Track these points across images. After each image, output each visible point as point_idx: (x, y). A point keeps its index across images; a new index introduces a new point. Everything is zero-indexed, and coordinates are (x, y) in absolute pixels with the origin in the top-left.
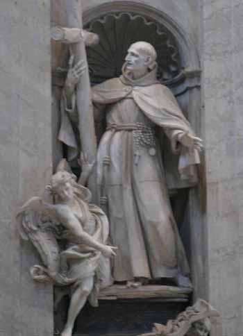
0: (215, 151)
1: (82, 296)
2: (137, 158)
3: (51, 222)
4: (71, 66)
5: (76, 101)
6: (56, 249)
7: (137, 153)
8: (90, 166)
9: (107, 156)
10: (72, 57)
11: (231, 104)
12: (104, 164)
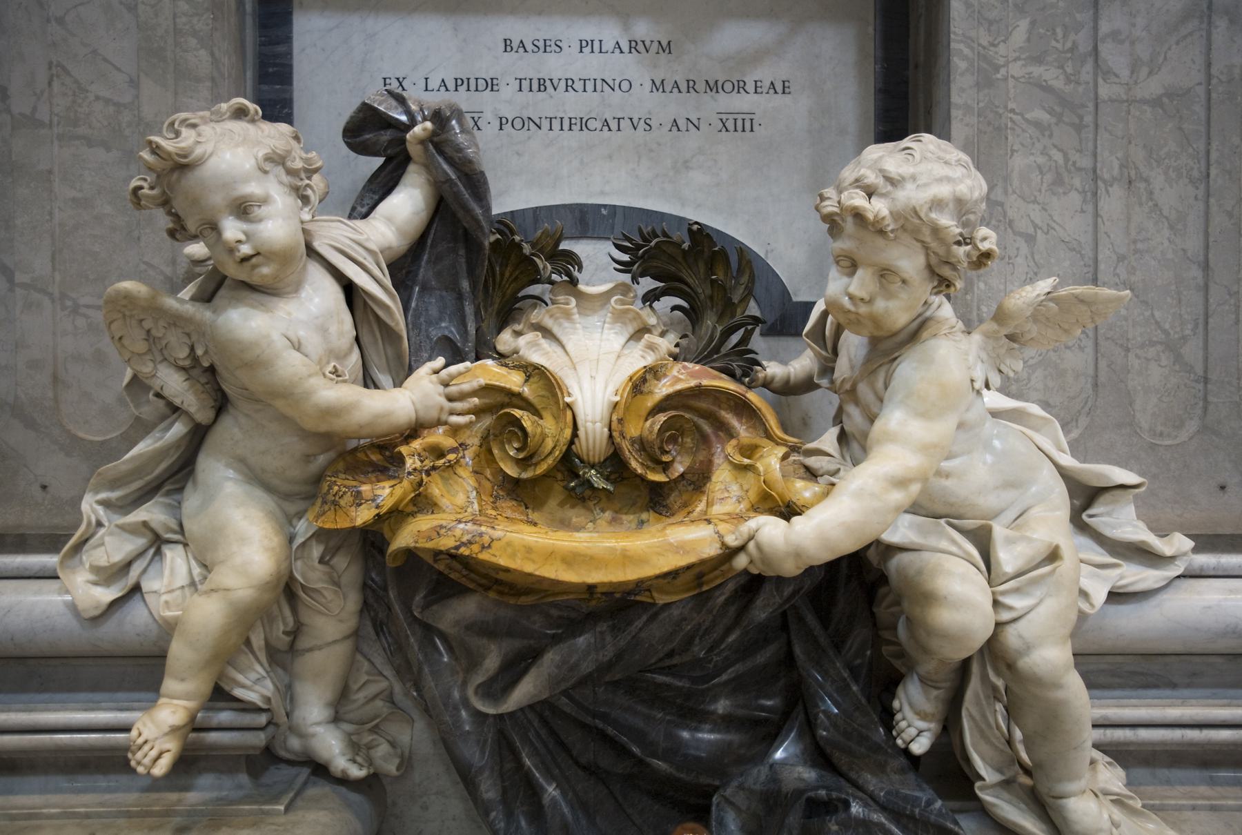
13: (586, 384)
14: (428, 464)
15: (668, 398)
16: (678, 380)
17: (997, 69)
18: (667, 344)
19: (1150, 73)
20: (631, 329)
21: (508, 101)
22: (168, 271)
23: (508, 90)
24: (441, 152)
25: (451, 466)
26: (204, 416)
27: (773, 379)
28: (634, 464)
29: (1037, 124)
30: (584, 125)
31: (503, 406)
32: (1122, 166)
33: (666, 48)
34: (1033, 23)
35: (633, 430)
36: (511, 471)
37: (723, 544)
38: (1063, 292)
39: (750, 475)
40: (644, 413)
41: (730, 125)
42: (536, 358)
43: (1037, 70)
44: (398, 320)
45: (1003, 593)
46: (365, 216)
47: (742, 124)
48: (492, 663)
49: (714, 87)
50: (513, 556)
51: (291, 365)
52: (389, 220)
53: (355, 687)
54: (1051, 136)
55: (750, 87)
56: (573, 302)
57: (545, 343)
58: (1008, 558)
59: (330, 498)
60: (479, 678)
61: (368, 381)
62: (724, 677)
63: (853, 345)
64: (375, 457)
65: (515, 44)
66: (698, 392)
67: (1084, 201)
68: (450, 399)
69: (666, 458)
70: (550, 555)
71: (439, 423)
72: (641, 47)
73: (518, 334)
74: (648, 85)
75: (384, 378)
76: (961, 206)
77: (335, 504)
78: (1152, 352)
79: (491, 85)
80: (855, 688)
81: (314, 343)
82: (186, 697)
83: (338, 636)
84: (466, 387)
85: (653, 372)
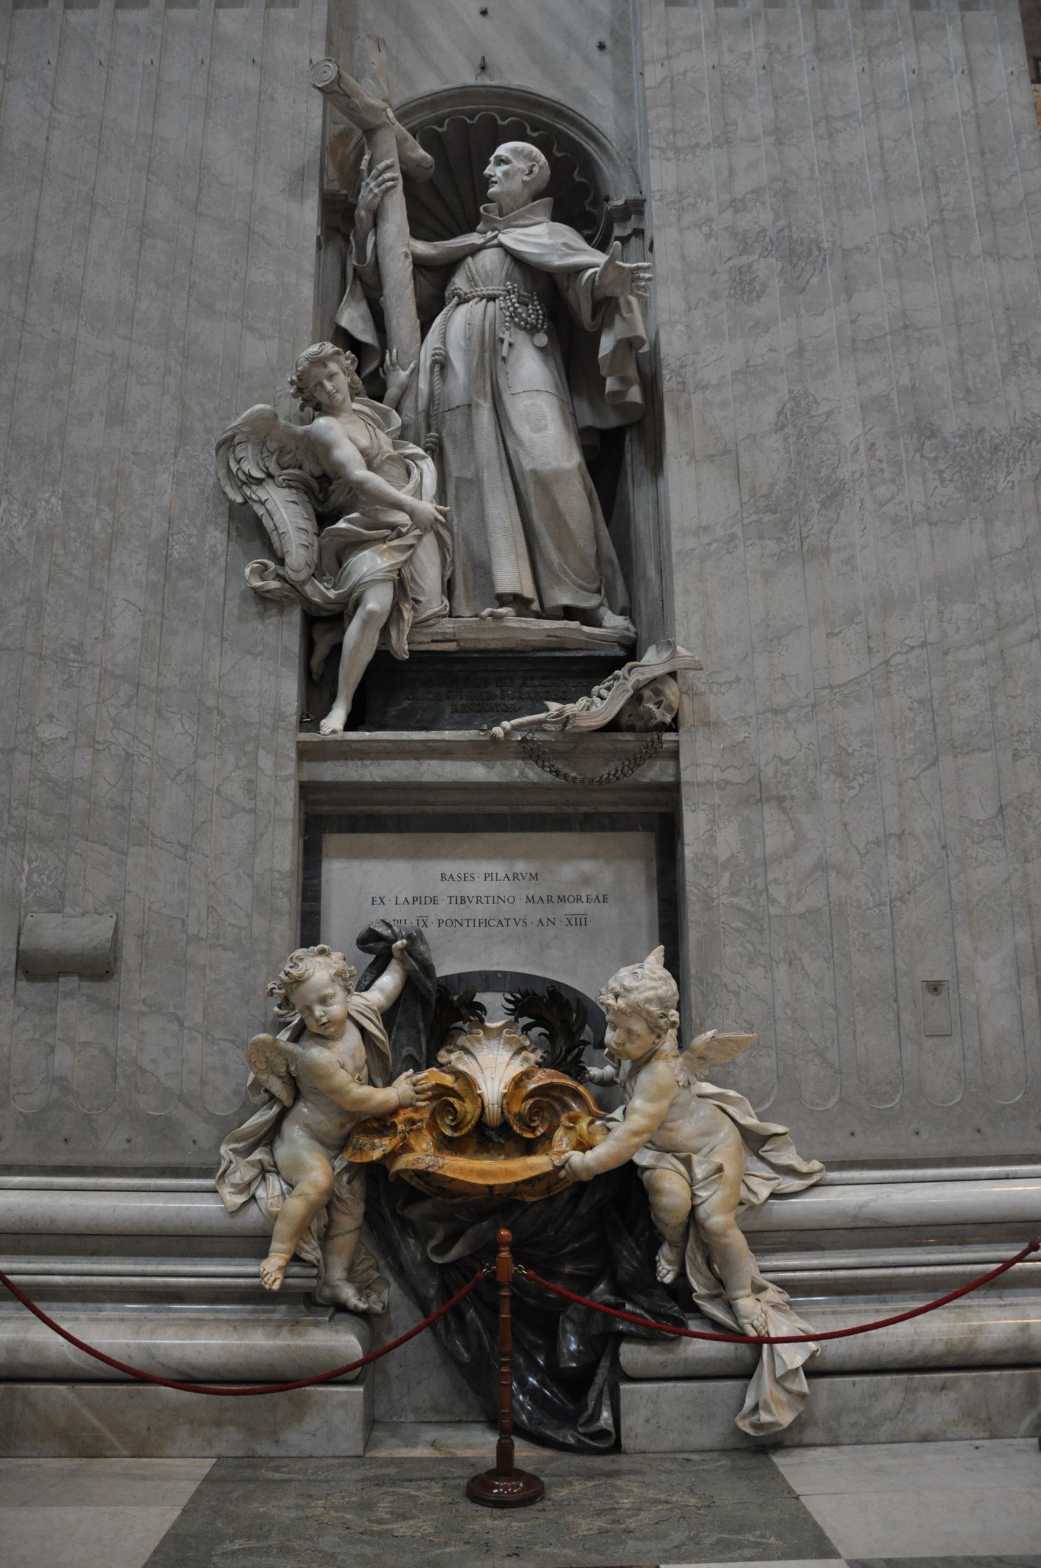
0: (679, 327)
1: (365, 624)
2: (506, 345)
3: (300, 468)
4: (365, 174)
5: (375, 245)
6: (311, 526)
7: (506, 336)
8: (403, 375)
9: (439, 345)
10: (367, 157)
11: (712, 241)
12: (434, 362)
13: (489, 1083)
14: (408, 1129)
15: (535, 1089)
16: (541, 1079)
17: (713, 900)
18: (535, 1057)
19: (798, 900)
20: (515, 1048)
21: (443, 909)
22: (263, 1020)
23: (443, 903)
24: (411, 955)
25: (420, 1129)
26: (288, 1103)
27: (594, 1076)
28: (515, 1128)
29: (737, 930)
30: (487, 923)
31: (442, 1095)
32: (785, 952)
33: (535, 877)
34: (732, 874)
35: (515, 1109)
36: (448, 1133)
37: (554, 1165)
38: (720, 1036)
39: (573, 1132)
40: (521, 1099)
41: (573, 922)
42: (461, 1067)
43: (735, 900)
44: (387, 1050)
45: (698, 1189)
46: (367, 988)
47: (581, 921)
48: (440, 1235)
49: (562, 899)
50: (454, 1171)
51: (342, 1078)
52: (381, 990)
53: (358, 1262)
54: (745, 936)
55: (584, 899)
56: (482, 1033)
57: (465, 1057)
58: (699, 1172)
59: (358, 1146)
60: (433, 1243)
61: (371, 1083)
62: (567, 1249)
63: (626, 1065)
64: (375, 1125)
65: (447, 877)
66: (551, 1086)
67: (766, 972)
68: (417, 1093)
69: (533, 1125)
70: (471, 1171)
71: (411, 1105)
72: (520, 877)
73: (450, 1052)
74: (524, 899)
75: (379, 1081)
76: (661, 1001)
77: (361, 1149)
78: (809, 1057)
79: (434, 900)
80: (638, 1252)
81: (350, 1064)
82: (285, 1252)
83: (353, 1228)
84: (425, 1086)
85: (526, 1075)
